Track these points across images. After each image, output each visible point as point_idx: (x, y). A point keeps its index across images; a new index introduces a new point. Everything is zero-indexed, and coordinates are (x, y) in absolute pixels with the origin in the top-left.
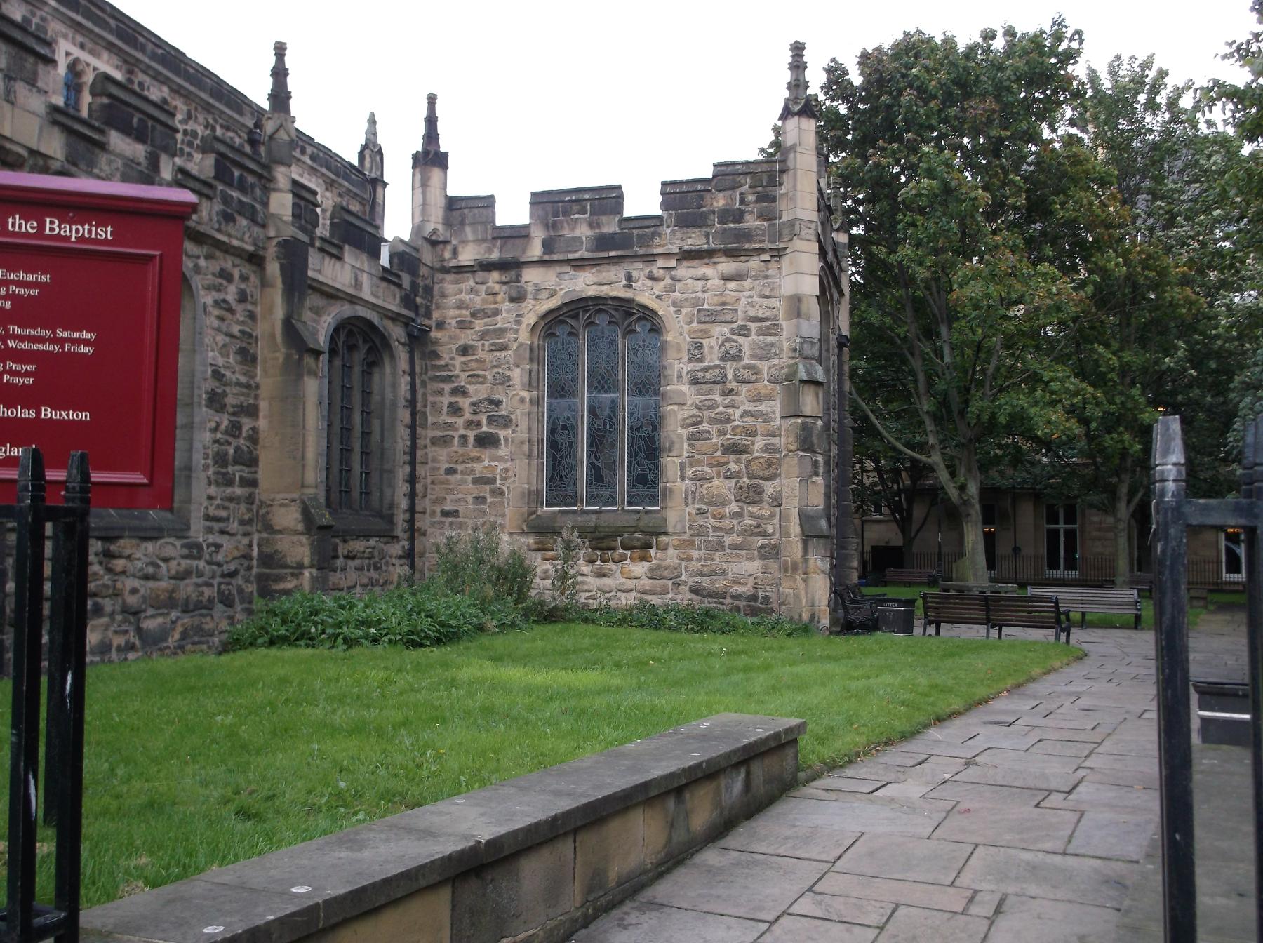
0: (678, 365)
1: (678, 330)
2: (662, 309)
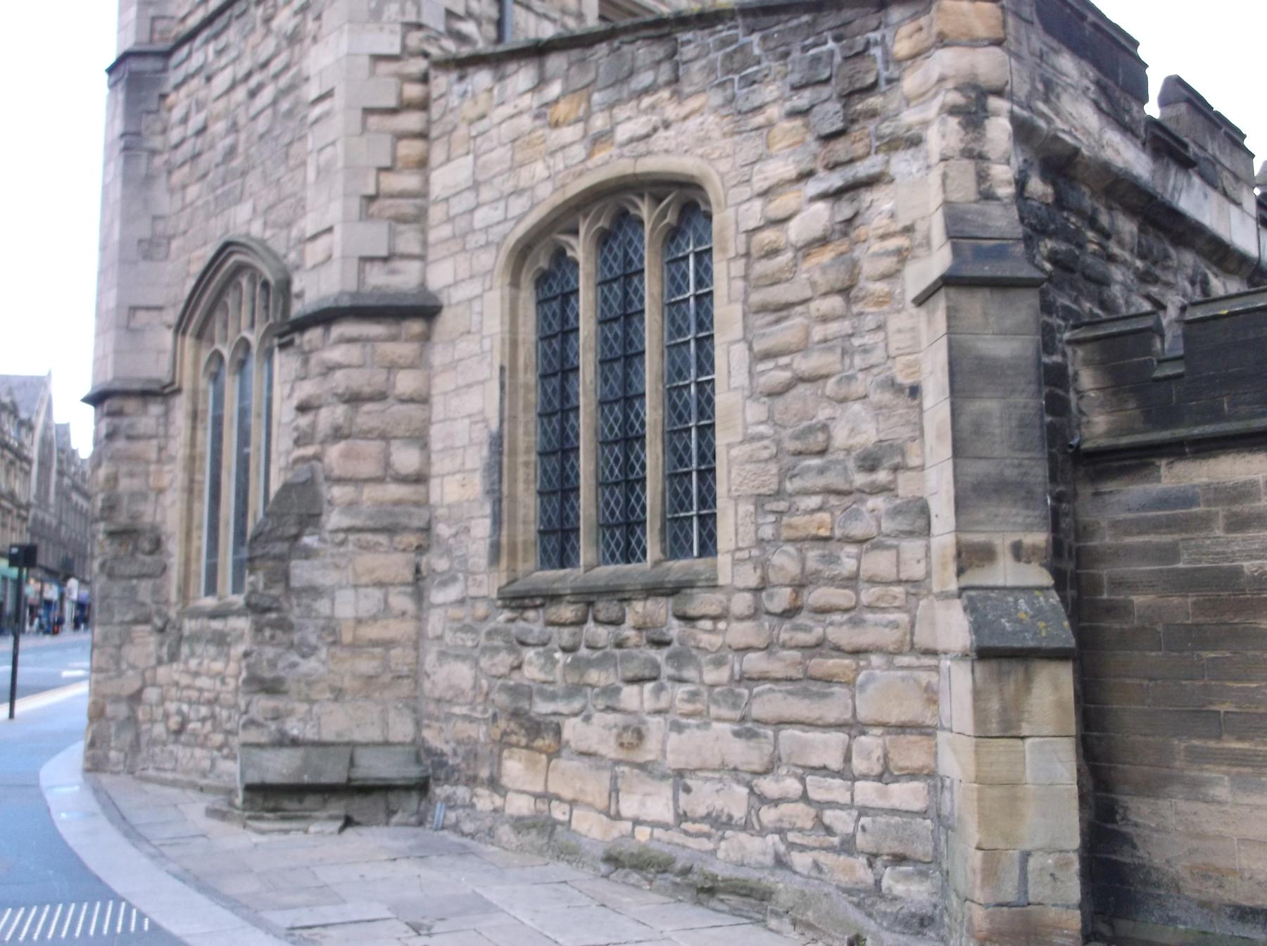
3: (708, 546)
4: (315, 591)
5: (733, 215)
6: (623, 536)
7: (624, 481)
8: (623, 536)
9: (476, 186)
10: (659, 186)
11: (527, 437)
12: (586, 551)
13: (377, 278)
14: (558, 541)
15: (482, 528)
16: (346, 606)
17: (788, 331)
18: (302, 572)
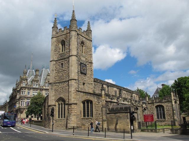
0: (165, 109)
1: (165, 107)
2: (164, 106)
3: (92, 117)
4: (71, 118)
5: (94, 103)
6: (88, 116)
7: (88, 114)
8: (88, 116)
9: (79, 98)
10: (90, 100)
11: (82, 111)
12: (86, 117)
13: (74, 102)
14: (84, 116)
15: (80, 115)
16: (73, 119)
17: (96, 108)
18: (70, 117)
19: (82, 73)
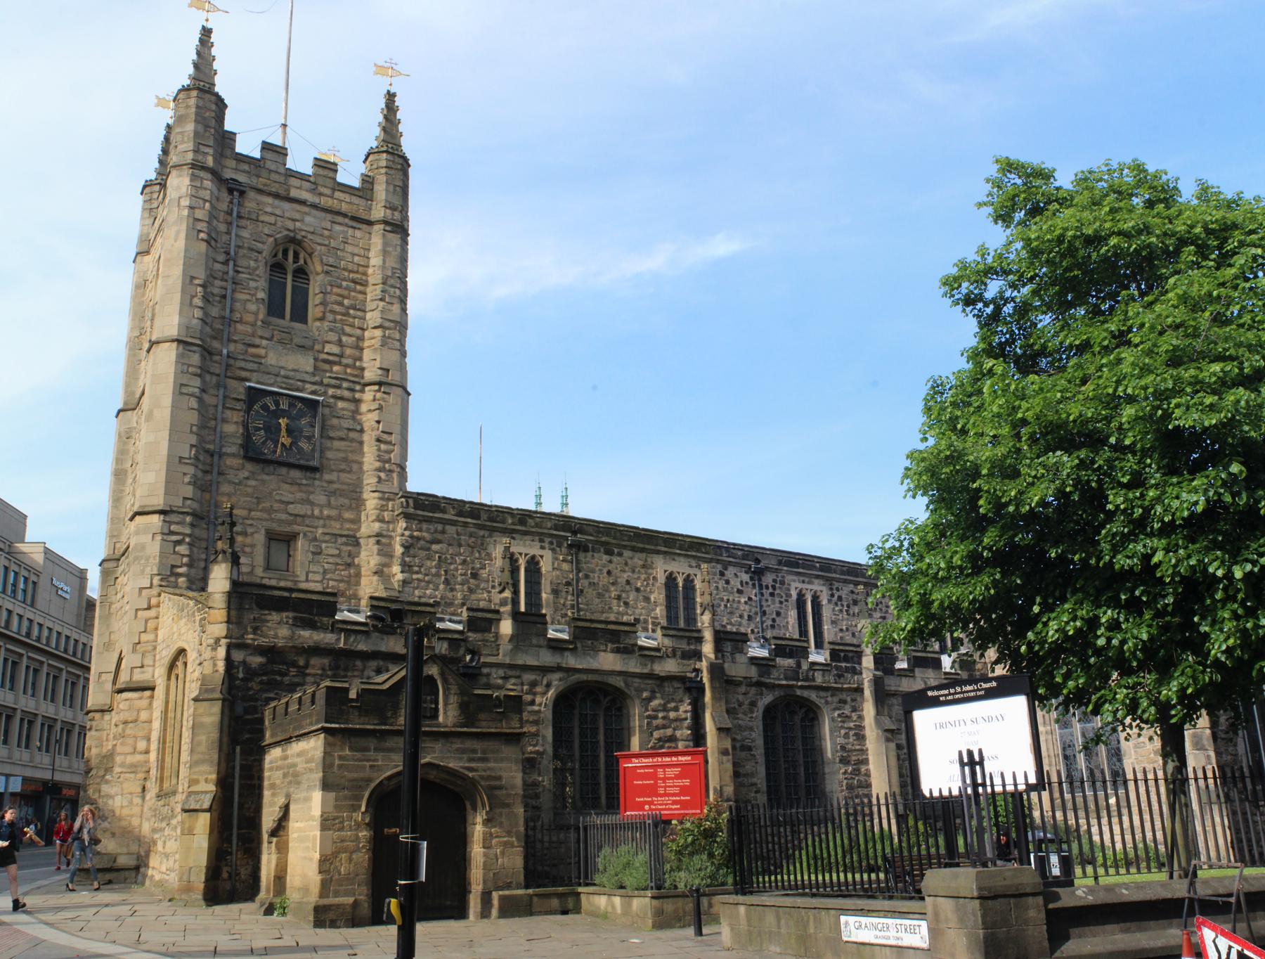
19: (251, 454)
